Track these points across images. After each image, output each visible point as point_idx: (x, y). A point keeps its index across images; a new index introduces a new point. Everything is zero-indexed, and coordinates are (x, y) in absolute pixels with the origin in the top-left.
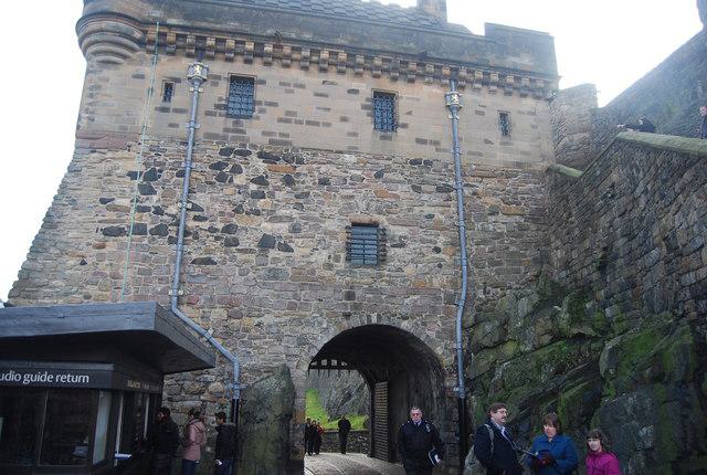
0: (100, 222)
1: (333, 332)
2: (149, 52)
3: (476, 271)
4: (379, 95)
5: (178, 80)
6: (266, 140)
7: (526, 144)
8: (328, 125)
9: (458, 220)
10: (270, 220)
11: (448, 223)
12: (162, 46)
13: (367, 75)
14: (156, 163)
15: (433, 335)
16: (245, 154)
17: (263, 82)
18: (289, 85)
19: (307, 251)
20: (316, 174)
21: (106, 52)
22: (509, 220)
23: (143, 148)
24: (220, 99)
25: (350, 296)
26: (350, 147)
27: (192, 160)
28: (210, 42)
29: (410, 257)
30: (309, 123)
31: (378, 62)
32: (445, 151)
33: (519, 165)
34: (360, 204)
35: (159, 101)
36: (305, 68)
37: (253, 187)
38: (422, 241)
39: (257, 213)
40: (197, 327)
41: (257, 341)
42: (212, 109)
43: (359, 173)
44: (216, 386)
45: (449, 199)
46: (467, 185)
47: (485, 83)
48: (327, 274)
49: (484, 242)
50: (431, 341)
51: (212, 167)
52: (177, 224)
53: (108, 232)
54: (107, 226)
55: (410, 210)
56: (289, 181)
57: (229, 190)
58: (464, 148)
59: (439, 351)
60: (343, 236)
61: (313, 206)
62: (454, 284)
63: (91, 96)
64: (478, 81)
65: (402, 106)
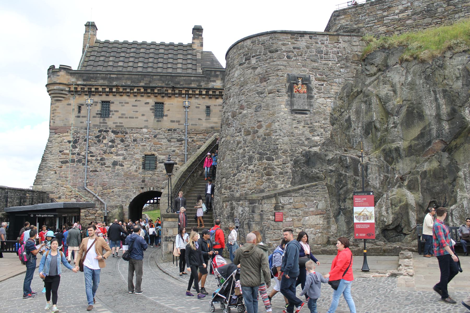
1: (138, 193)
2: (72, 95)
5: (83, 105)
8: (137, 118)
10: (116, 156)
11: (181, 153)
13: (152, 96)
16: (107, 131)
17: (113, 103)
18: (122, 103)
19: (129, 166)
23: (72, 132)
24: (98, 111)
25: (143, 181)
26: (145, 126)
27: (89, 135)
28: (93, 90)
30: (130, 118)
31: (156, 91)
33: (212, 128)
35: (77, 114)
36: (129, 96)
37: (110, 144)
39: (112, 153)
40: (93, 193)
42: (95, 115)
43: (148, 136)
44: (99, 212)
45: (182, 144)
46: (190, 138)
47: (200, 94)
52: (85, 159)
54: (62, 160)
55: (166, 149)
56: (122, 141)
57: (102, 145)
58: (190, 123)
60: (141, 160)
61: (131, 150)
64: (197, 94)
65: (166, 107)
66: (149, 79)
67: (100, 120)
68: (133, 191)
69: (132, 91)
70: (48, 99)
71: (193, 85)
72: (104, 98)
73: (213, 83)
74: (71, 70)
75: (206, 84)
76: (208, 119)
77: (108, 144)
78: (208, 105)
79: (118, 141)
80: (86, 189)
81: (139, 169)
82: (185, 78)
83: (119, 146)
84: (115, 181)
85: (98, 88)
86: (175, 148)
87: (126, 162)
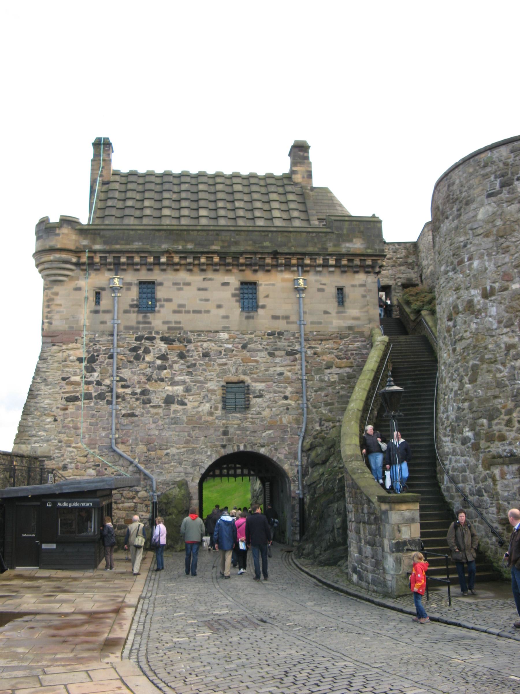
0: (63, 393)
1: (215, 457)
2: (83, 270)
3: (314, 410)
5: (103, 289)
6: (165, 327)
7: (357, 311)
8: (208, 312)
9: (301, 375)
11: (294, 377)
12: (91, 266)
13: (235, 270)
14: (94, 351)
15: (282, 457)
16: (151, 339)
17: (161, 284)
19: (196, 404)
20: (200, 349)
21: (55, 275)
23: (85, 340)
24: (133, 300)
25: (225, 433)
26: (224, 327)
27: (118, 346)
28: (123, 260)
29: (267, 404)
30: (195, 312)
31: (242, 261)
32: (293, 323)
33: (350, 328)
34: (231, 369)
36: (190, 270)
37: (159, 362)
38: (275, 392)
39: (162, 380)
40: (129, 458)
41: (166, 466)
42: (128, 308)
43: (230, 346)
44: (142, 494)
45: (295, 360)
46: (309, 348)
47: (325, 265)
48: (210, 419)
49: (321, 389)
50: (281, 460)
52: (111, 391)
53: (68, 400)
55: (266, 370)
56: (182, 356)
57: (143, 366)
58: (308, 319)
59: (286, 467)
60: (219, 392)
62: (298, 421)
63: (48, 306)
64: (319, 266)
65: (262, 290)
67: (137, 316)
68: (206, 452)
69: (196, 262)
70: (37, 281)
71: (310, 249)
72: (144, 276)
73: (347, 245)
74: (79, 223)
77: (154, 362)
78: (341, 284)
79: (173, 357)
80: (114, 451)
81: (216, 409)
83: (176, 366)
84: (171, 433)
86: (283, 369)
87: (191, 398)
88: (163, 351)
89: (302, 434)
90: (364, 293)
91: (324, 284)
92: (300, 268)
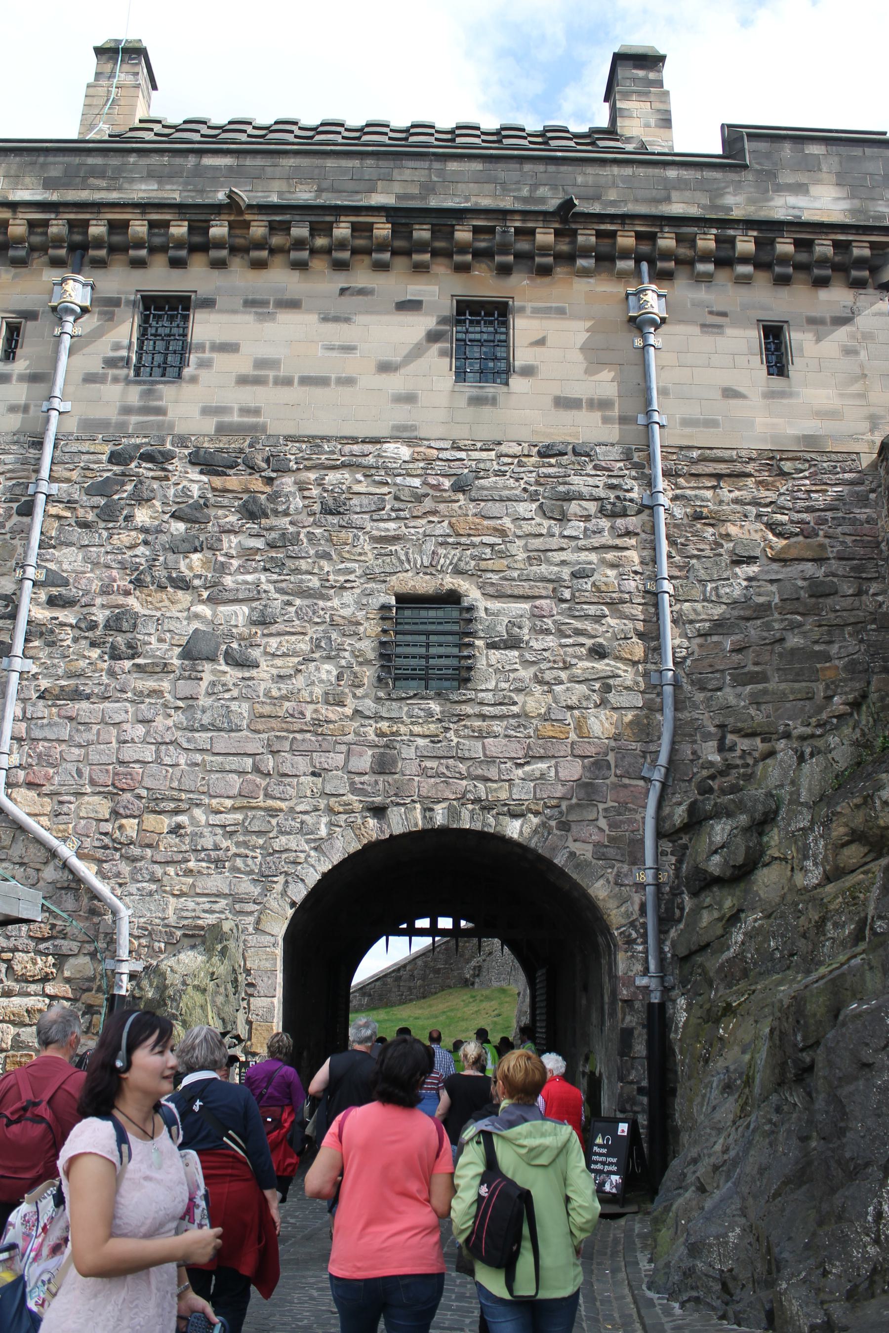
1: (344, 846)
3: (699, 697)
4: (468, 310)
5: (31, 315)
6: (209, 425)
8: (349, 381)
13: (441, 269)
15: (585, 851)
22: (784, 573)
24: (117, 347)
26: (396, 428)
28: (97, 230)
30: (305, 381)
31: (463, 235)
36: (300, 266)
37: (179, 527)
47: (725, 260)
48: (332, 713)
50: (581, 865)
51: (89, 492)
57: (125, 538)
59: (599, 891)
60: (371, 628)
64: (705, 257)
66: (421, 176)
69: (321, 242)
71: (677, 209)
72: (159, 279)
75: (751, 201)
76: (782, 394)
82: (628, 171)
85: (125, 224)
87: (274, 642)
88: (196, 494)
89: (658, 775)
90: (851, 343)
91: (724, 314)
92: (645, 266)
